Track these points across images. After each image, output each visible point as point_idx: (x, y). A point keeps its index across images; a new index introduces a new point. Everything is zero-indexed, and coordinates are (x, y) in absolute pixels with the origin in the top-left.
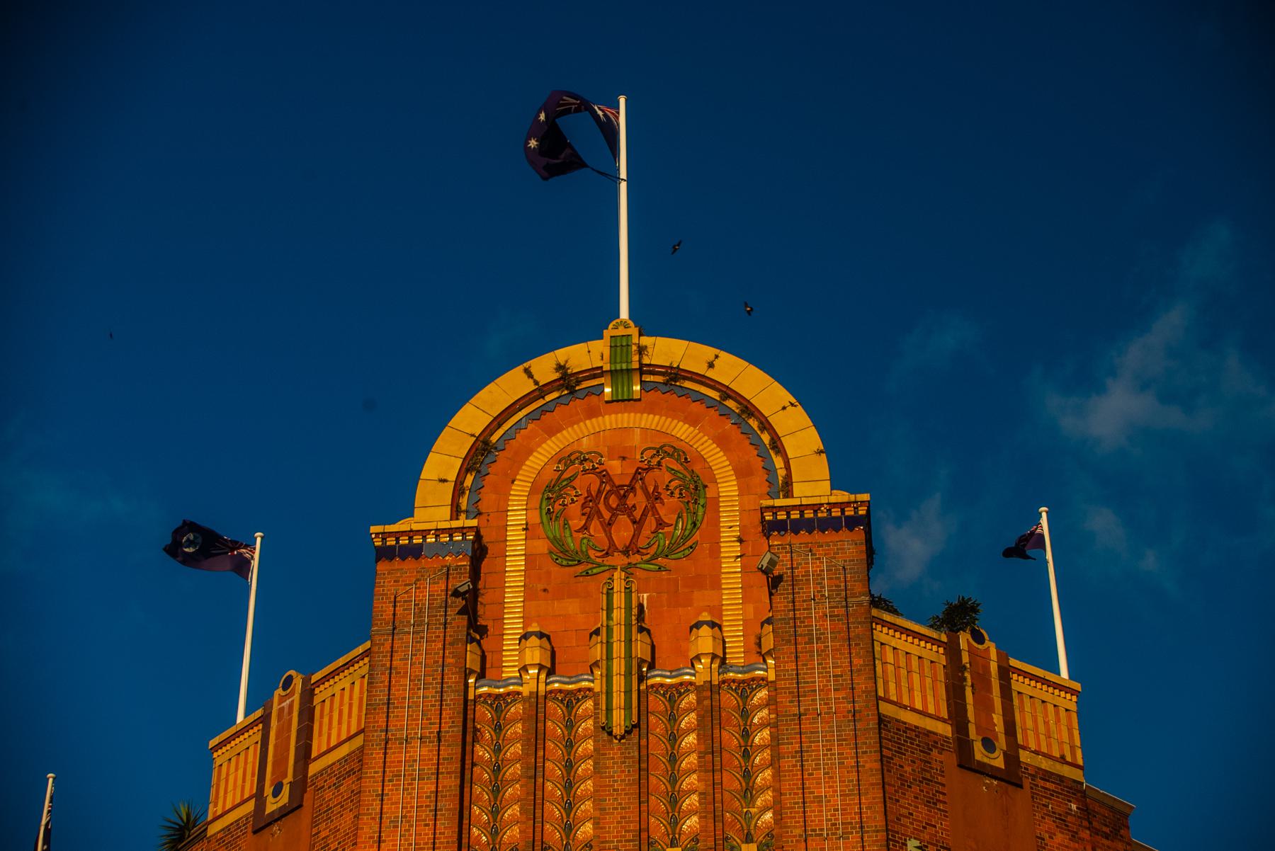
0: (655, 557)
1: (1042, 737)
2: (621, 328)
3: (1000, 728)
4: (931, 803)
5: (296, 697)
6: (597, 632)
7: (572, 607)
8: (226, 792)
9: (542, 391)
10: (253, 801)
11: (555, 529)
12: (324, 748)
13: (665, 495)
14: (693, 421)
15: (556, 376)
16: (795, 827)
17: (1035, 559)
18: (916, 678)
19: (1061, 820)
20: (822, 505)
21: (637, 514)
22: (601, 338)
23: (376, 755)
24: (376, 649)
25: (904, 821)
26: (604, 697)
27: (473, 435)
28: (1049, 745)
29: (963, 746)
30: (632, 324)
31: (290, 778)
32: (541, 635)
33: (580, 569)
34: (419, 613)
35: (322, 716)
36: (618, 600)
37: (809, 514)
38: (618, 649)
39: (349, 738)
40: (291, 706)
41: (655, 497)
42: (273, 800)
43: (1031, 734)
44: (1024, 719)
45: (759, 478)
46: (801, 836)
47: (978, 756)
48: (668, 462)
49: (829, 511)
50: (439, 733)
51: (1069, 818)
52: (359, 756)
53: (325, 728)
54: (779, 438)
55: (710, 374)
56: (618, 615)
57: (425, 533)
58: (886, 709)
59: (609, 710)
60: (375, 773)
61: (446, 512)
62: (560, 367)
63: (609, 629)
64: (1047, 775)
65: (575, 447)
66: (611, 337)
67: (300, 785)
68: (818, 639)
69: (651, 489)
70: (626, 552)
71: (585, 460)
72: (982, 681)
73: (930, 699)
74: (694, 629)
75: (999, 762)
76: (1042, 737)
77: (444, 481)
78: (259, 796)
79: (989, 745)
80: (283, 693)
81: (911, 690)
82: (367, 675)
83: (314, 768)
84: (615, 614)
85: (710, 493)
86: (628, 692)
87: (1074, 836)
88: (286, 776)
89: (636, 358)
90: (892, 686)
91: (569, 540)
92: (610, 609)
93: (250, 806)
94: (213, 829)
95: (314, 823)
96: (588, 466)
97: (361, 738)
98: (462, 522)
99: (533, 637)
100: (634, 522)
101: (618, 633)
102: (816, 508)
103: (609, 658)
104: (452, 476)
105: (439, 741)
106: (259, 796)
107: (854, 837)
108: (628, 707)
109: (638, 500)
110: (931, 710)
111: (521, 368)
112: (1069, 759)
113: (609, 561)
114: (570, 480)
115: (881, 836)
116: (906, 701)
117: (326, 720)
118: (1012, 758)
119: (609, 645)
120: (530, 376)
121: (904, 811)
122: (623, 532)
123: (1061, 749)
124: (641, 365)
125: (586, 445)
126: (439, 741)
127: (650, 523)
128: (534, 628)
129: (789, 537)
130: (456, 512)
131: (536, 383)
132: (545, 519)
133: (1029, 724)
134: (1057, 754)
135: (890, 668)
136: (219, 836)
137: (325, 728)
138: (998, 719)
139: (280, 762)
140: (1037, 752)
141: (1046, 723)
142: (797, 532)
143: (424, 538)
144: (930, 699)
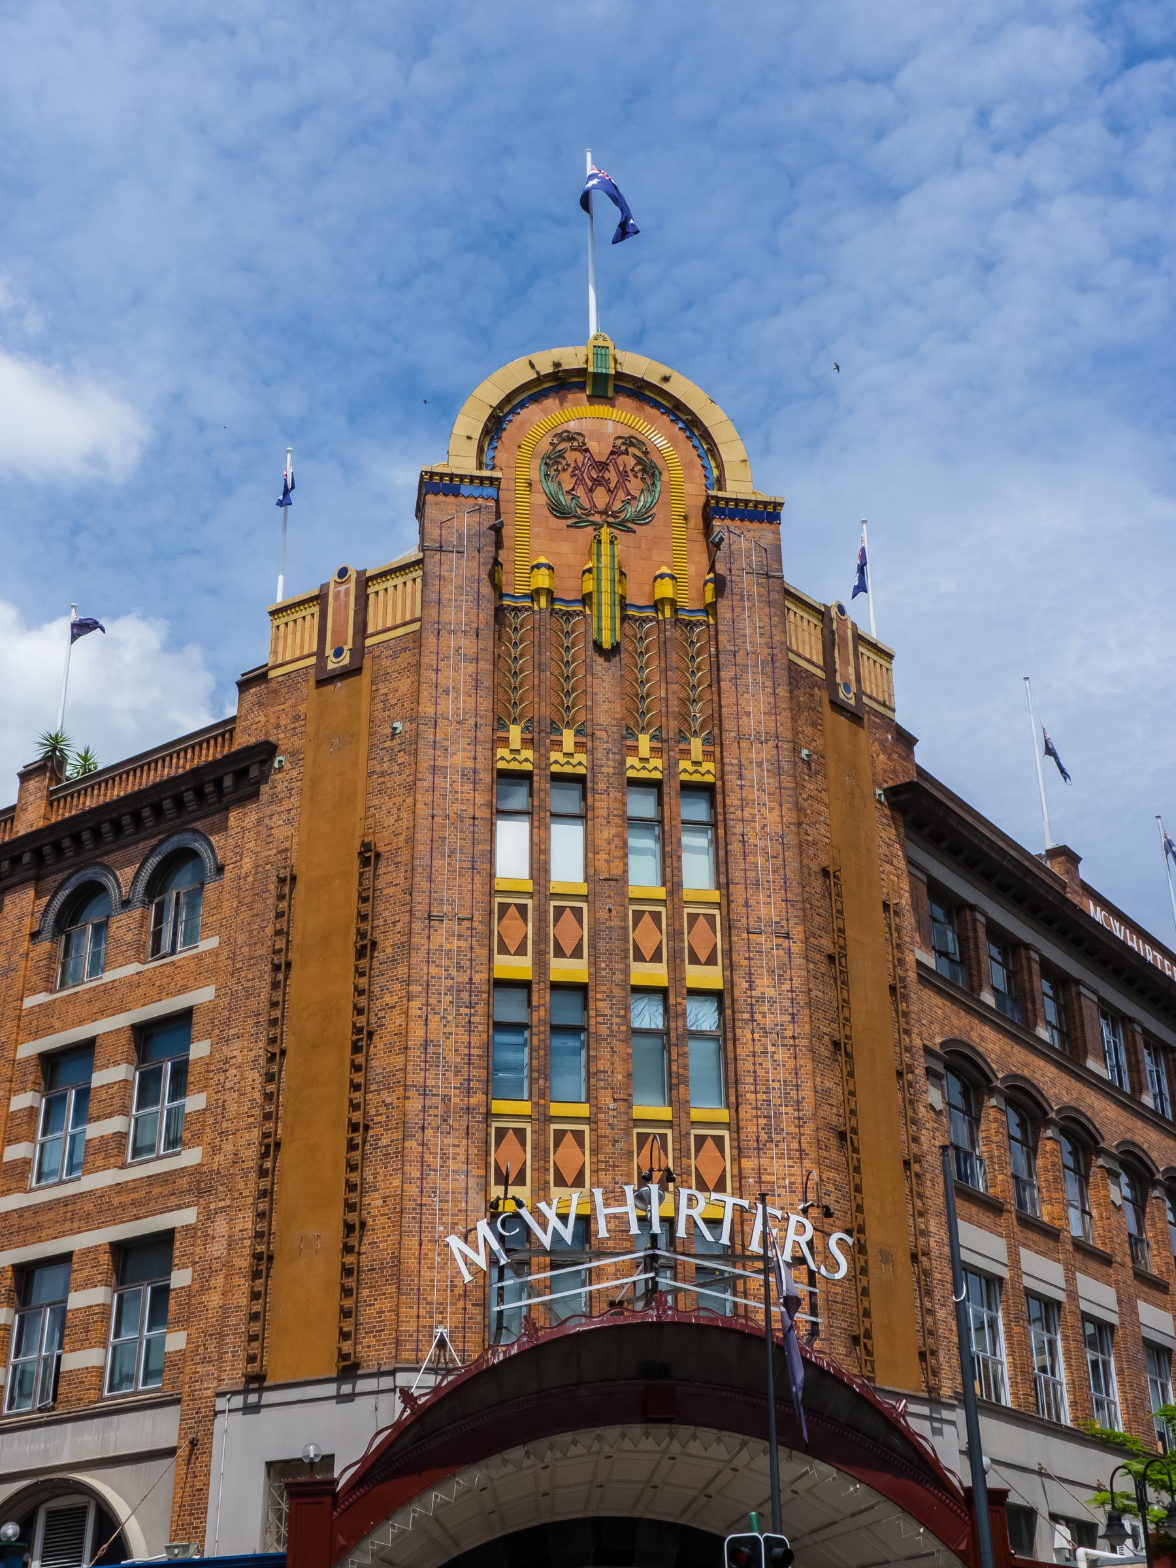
0: (625, 521)
1: (874, 686)
2: (601, 340)
3: (853, 677)
4: (814, 725)
5: (352, 586)
6: (590, 571)
7: (565, 548)
8: (285, 648)
9: (540, 379)
10: (315, 658)
11: (553, 487)
12: (380, 627)
13: (631, 474)
14: (651, 421)
15: (550, 370)
16: (732, 731)
17: (863, 557)
18: (806, 634)
19: (883, 745)
20: (751, 501)
21: (612, 486)
22: (585, 344)
23: (430, 641)
24: (427, 560)
25: (800, 735)
26: (595, 619)
27: (491, 406)
28: (877, 692)
29: (831, 685)
30: (608, 338)
31: (350, 645)
32: (550, 568)
33: (570, 522)
34: (460, 537)
35: (376, 603)
36: (605, 548)
37: (742, 506)
38: (606, 585)
39: (405, 624)
40: (347, 591)
41: (624, 475)
42: (335, 660)
43: (868, 683)
44: (865, 673)
45: (699, 472)
46: (735, 738)
47: (841, 696)
48: (632, 450)
49: (756, 506)
50: (477, 629)
51: (887, 745)
52: (417, 637)
53: (380, 613)
54: (716, 445)
55: (666, 387)
56: (605, 560)
57: (462, 477)
58: (792, 656)
59: (600, 630)
60: (431, 652)
61: (473, 462)
62: (557, 365)
63: (599, 570)
64: (877, 713)
65: (565, 427)
66: (594, 346)
67: (359, 651)
68: (748, 599)
69: (621, 469)
70: (603, 513)
71: (573, 439)
72: (844, 639)
73: (814, 651)
74: (659, 580)
75: (852, 702)
76: (874, 686)
77: (469, 438)
78: (320, 653)
79: (847, 687)
80: (340, 580)
81: (804, 643)
82: (419, 581)
83: (369, 642)
84: (603, 559)
85: (665, 476)
86: (613, 618)
87: (890, 758)
88: (346, 643)
89: (612, 364)
90: (793, 639)
91: (561, 498)
92: (599, 555)
93: (313, 660)
94: (272, 674)
95: (373, 682)
96: (575, 444)
97: (419, 623)
98: (486, 473)
99: (543, 569)
100: (609, 490)
101: (605, 574)
102: (746, 502)
103: (599, 591)
104: (476, 435)
105: (477, 636)
106: (320, 653)
107: (772, 744)
108: (613, 630)
109: (612, 476)
110: (815, 659)
111: (522, 361)
112: (887, 703)
113: (591, 518)
114: (563, 451)
115: (790, 745)
116: (801, 652)
117: (381, 606)
118: (858, 697)
119: (598, 580)
120: (532, 365)
121: (800, 729)
122: (601, 498)
123: (884, 696)
124: (617, 372)
125: (573, 426)
126: (477, 636)
127: (621, 495)
128: (542, 560)
129: (728, 522)
130: (480, 465)
131: (538, 373)
132: (543, 479)
133: (867, 675)
134: (881, 699)
135: (793, 626)
136: (280, 679)
137: (380, 613)
138: (851, 670)
139: (339, 633)
140: (870, 697)
141: (876, 676)
142: (732, 519)
143: (462, 481)
144: (814, 651)
